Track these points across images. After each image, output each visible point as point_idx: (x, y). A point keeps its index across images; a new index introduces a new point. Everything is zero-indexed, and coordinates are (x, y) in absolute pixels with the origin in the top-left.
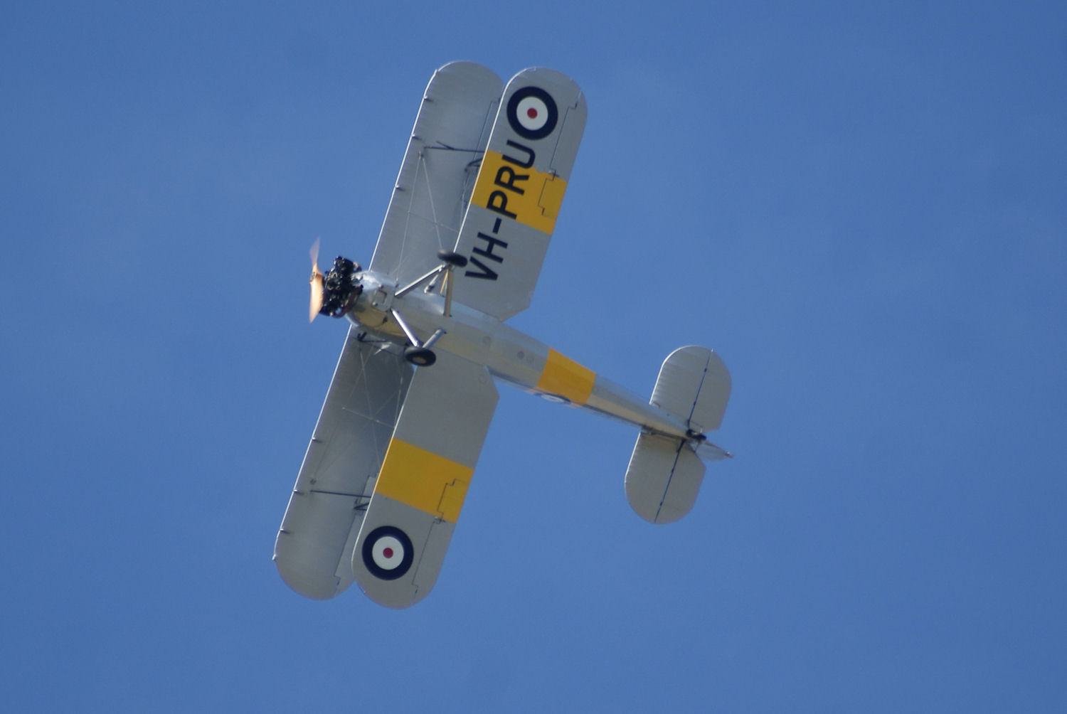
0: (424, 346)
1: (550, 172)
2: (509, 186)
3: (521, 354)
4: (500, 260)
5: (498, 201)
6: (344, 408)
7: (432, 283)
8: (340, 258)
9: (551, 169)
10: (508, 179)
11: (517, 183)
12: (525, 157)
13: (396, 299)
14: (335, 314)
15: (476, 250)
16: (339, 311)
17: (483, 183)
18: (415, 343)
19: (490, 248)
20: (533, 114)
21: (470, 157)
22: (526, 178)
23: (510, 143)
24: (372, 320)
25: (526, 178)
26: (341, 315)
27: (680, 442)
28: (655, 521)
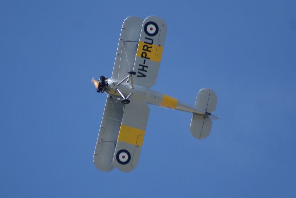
0: (127, 98)
1: (158, 45)
2: (147, 50)
3: (155, 97)
4: (146, 71)
5: (144, 55)
6: (108, 118)
7: (128, 80)
8: (101, 76)
9: (158, 44)
10: (146, 48)
11: (149, 49)
12: (150, 42)
13: (118, 86)
14: (102, 92)
15: (139, 69)
16: (102, 91)
17: (139, 51)
18: (124, 98)
19: (143, 68)
20: (151, 29)
21: (136, 43)
22: (151, 47)
23: (146, 38)
24: (112, 93)
25: (151, 47)
26: (103, 92)
27: (204, 116)
28: (200, 138)
